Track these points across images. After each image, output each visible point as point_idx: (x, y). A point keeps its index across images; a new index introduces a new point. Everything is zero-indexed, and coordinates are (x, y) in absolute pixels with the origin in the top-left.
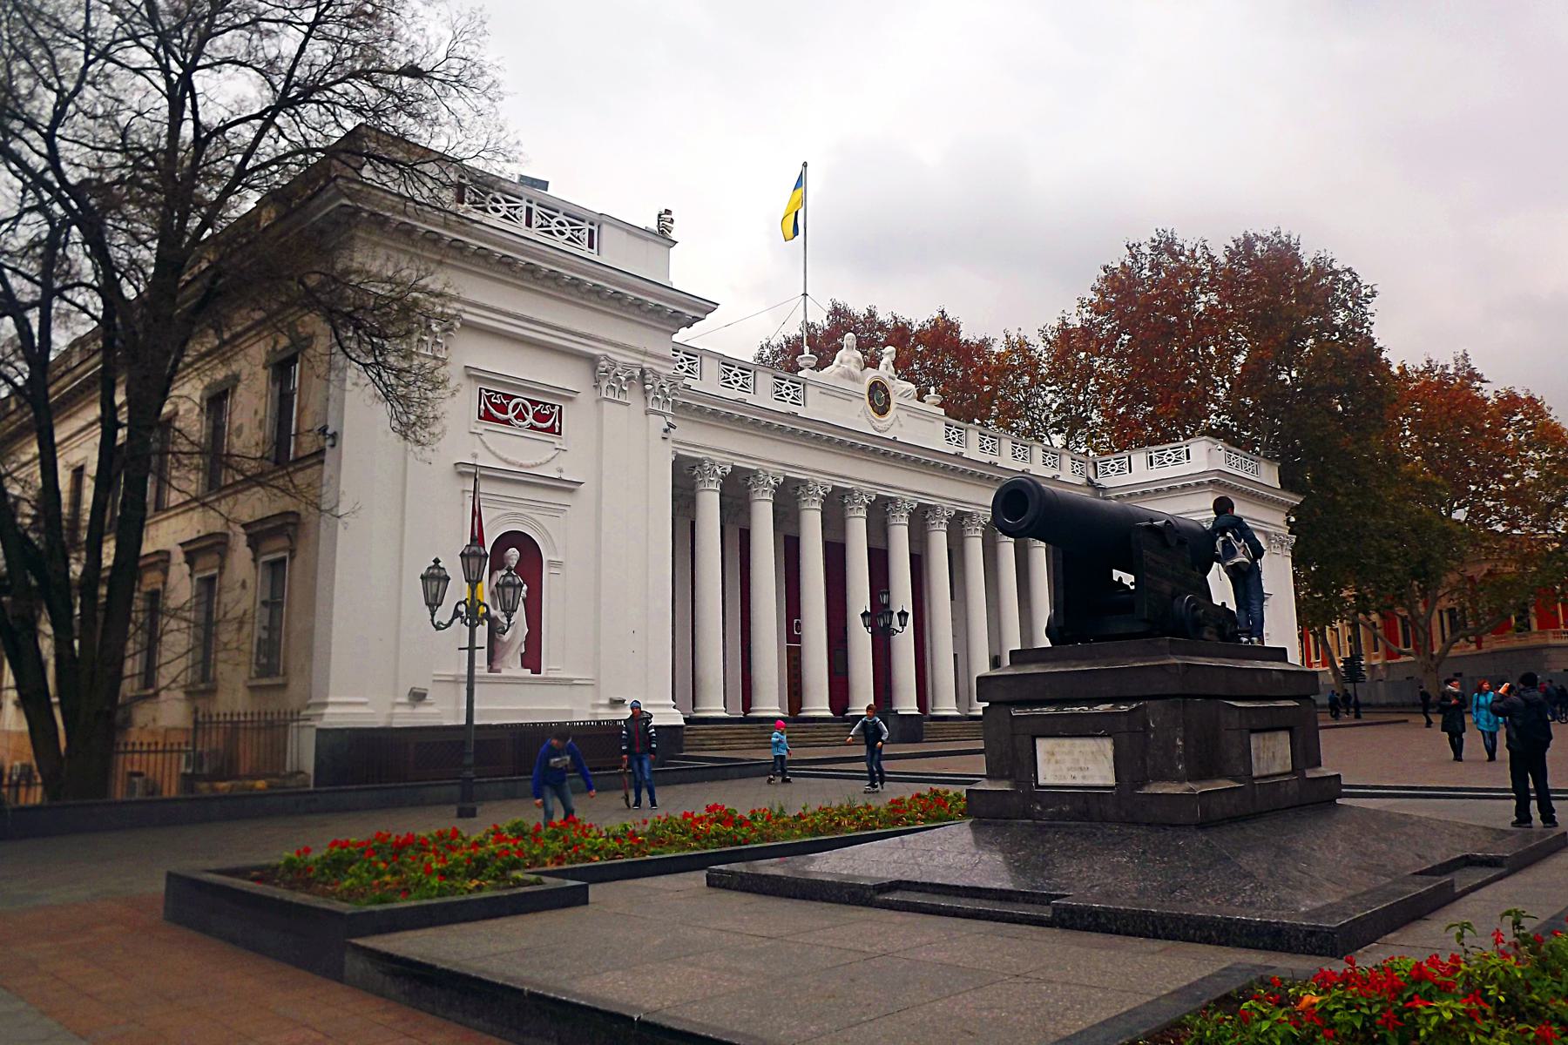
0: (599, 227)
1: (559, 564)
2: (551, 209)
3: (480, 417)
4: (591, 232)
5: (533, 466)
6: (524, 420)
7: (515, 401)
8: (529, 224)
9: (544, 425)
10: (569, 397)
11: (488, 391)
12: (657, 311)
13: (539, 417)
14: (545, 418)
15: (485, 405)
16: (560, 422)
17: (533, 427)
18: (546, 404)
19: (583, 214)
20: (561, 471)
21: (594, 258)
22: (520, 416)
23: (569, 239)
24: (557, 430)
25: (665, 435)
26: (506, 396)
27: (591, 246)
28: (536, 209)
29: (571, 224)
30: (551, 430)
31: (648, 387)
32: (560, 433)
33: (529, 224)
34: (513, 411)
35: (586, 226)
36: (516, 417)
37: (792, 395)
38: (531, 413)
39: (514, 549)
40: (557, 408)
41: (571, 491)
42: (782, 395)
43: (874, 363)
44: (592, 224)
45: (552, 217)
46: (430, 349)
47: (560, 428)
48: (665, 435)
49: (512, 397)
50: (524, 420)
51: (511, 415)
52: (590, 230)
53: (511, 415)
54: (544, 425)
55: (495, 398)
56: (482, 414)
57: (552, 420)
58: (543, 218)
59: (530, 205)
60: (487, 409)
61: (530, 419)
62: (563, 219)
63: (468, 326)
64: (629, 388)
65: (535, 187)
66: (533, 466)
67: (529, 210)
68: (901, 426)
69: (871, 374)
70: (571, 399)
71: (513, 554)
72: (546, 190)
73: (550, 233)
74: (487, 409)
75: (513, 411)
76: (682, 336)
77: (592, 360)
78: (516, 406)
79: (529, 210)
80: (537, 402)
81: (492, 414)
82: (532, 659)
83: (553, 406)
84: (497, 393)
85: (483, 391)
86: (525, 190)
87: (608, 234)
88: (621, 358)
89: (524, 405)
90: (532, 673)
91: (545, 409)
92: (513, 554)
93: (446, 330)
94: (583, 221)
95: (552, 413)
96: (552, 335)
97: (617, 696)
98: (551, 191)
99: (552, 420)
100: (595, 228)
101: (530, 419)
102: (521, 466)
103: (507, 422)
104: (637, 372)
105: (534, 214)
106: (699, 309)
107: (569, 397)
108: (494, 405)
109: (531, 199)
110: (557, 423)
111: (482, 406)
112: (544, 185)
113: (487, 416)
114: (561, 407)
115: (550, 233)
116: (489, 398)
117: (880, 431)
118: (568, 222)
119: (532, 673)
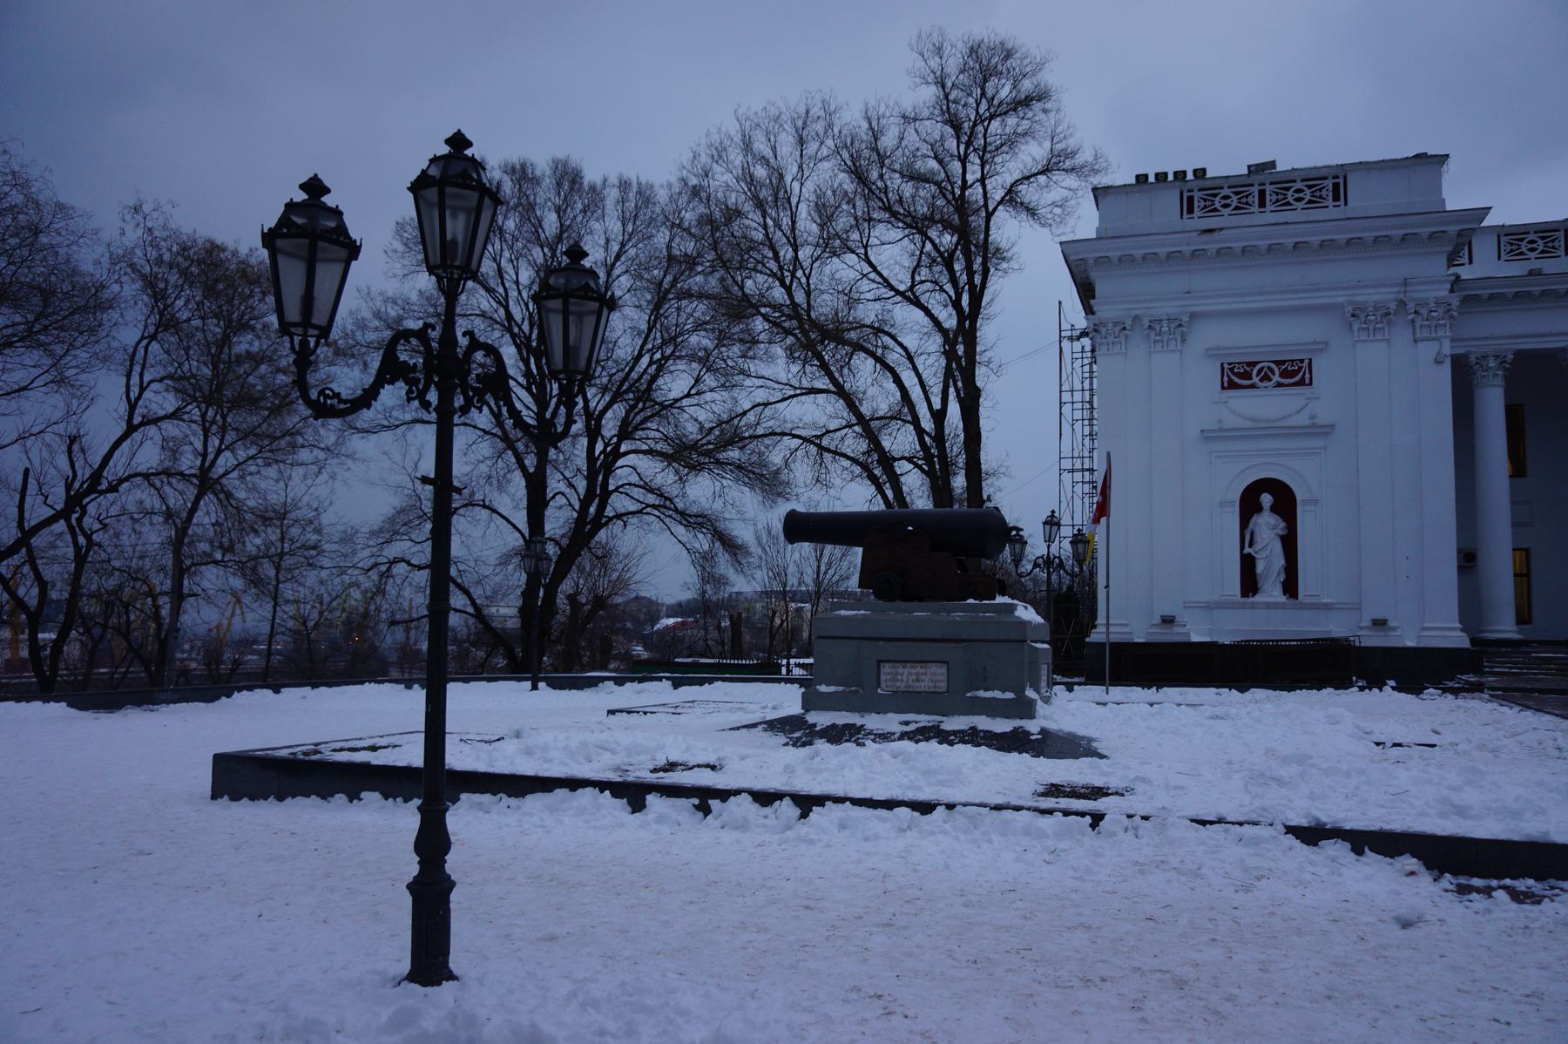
1: (1315, 502)
2: (1286, 183)
3: (1223, 388)
4: (1336, 186)
6: (1270, 380)
8: (1262, 204)
11: (1230, 364)
13: (1285, 374)
14: (1292, 374)
15: (1228, 376)
16: (1310, 373)
17: (1279, 385)
18: (1293, 361)
19: (1323, 173)
22: (1266, 378)
24: (1307, 381)
27: (1336, 198)
28: (1269, 189)
30: (1301, 383)
32: (1311, 384)
33: (1262, 204)
34: (1257, 376)
35: (1329, 183)
38: (1277, 373)
39: (1266, 494)
40: (1307, 361)
41: (1326, 434)
47: (1311, 379)
49: (1254, 364)
50: (1270, 380)
51: (1255, 380)
53: (1255, 380)
56: (1226, 385)
60: (1230, 381)
61: (1276, 378)
67: (1262, 193)
70: (1321, 350)
71: (1266, 499)
74: (1230, 381)
78: (1262, 369)
79: (1262, 193)
80: (1283, 362)
81: (1236, 383)
82: (1290, 586)
83: (1302, 361)
84: (1239, 363)
85: (1225, 365)
86: (1256, 179)
89: (1269, 368)
92: (1266, 499)
95: (1300, 369)
101: (1276, 378)
102: (1268, 421)
103: (1253, 386)
105: (1268, 193)
108: (1237, 375)
110: (1307, 376)
111: (1226, 379)
112: (1272, 164)
113: (1232, 386)
114: (1310, 360)
116: (1231, 370)
118: (1306, 186)
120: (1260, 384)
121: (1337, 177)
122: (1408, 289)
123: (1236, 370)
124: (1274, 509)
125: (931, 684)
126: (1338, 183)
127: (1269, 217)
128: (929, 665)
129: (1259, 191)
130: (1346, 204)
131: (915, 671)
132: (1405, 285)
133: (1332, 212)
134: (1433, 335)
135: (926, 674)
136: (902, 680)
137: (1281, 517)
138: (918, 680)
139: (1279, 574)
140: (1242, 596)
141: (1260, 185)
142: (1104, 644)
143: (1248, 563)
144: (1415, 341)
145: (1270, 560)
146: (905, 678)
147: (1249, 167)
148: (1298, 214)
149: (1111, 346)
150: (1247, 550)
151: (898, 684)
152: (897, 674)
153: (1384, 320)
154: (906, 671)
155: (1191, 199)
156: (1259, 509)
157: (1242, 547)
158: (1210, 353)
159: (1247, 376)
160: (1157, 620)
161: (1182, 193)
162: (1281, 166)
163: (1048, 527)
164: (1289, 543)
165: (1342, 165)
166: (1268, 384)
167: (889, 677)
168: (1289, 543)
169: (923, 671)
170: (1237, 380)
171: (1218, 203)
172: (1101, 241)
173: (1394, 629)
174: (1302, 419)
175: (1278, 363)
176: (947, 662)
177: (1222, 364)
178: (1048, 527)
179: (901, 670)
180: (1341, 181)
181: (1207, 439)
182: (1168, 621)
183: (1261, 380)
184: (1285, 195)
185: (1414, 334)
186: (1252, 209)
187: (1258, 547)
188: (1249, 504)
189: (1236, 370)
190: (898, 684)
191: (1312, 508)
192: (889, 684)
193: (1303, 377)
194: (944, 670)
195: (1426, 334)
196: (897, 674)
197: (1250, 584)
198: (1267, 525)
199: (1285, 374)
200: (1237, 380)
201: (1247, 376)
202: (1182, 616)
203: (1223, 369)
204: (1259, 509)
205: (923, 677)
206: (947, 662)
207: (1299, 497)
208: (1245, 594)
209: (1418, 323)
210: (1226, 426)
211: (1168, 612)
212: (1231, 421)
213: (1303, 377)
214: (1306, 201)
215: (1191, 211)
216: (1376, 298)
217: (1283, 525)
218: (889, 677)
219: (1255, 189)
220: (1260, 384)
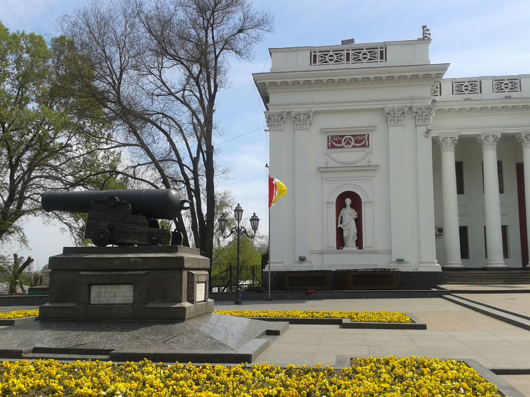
1: (370, 202)
2: (358, 50)
3: (328, 148)
4: (382, 52)
6: (350, 144)
7: (345, 137)
8: (348, 60)
9: (360, 145)
10: (373, 128)
11: (331, 136)
13: (357, 141)
14: (360, 141)
15: (331, 142)
16: (368, 141)
17: (354, 147)
19: (376, 46)
20: (370, 162)
22: (348, 143)
24: (367, 145)
25: (426, 135)
26: (341, 136)
27: (382, 58)
28: (351, 52)
30: (364, 146)
32: (368, 146)
33: (348, 60)
34: (344, 142)
35: (379, 50)
36: (346, 144)
38: (353, 141)
40: (367, 135)
45: (360, 53)
47: (368, 144)
48: (426, 135)
49: (342, 137)
50: (350, 144)
51: (343, 144)
52: (381, 51)
53: (343, 144)
54: (360, 145)
55: (336, 138)
56: (330, 146)
60: (332, 144)
61: (353, 143)
63: (315, 113)
64: (404, 118)
66: (355, 163)
67: (348, 54)
70: (374, 130)
71: (348, 201)
74: (332, 144)
75: (344, 142)
79: (348, 54)
80: (356, 136)
82: (359, 243)
83: (365, 135)
84: (336, 136)
85: (330, 137)
88: (395, 105)
89: (349, 138)
91: (360, 138)
92: (348, 201)
95: (364, 139)
96: (369, 105)
97: (400, 258)
98: (356, 42)
100: (384, 50)
101: (353, 143)
102: (349, 164)
103: (342, 147)
104: (406, 110)
105: (350, 55)
106: (444, 67)
107: (373, 128)
108: (335, 141)
110: (367, 142)
111: (330, 143)
112: (352, 41)
113: (333, 147)
114: (368, 135)
116: (332, 139)
121: (382, 48)
123: (334, 139)
124: (352, 206)
126: (383, 51)
127: (351, 65)
129: (347, 53)
130: (386, 61)
133: (379, 64)
134: (424, 123)
137: (355, 210)
139: (354, 237)
143: (340, 232)
145: (350, 231)
147: (342, 41)
148: (365, 64)
150: (339, 226)
153: (402, 115)
155: (315, 56)
156: (345, 206)
157: (337, 224)
158: (323, 131)
159: (339, 142)
160: (297, 259)
161: (311, 53)
165: (384, 42)
168: (358, 222)
171: (327, 58)
172: (271, 74)
174: (364, 163)
175: (354, 136)
177: (328, 136)
180: (384, 50)
181: (322, 172)
182: (302, 259)
183: (346, 144)
185: (416, 123)
186: (343, 62)
187: (344, 223)
188: (340, 203)
189: (334, 139)
191: (369, 205)
193: (365, 144)
195: (421, 123)
197: (341, 242)
198: (349, 214)
199: (357, 141)
201: (339, 142)
202: (309, 258)
204: (345, 206)
207: (363, 200)
208: (338, 248)
209: (417, 118)
210: (329, 166)
211: (303, 255)
212: (331, 164)
213: (365, 144)
214: (368, 59)
215: (315, 62)
216: (400, 105)
217: (356, 213)
219: (345, 53)
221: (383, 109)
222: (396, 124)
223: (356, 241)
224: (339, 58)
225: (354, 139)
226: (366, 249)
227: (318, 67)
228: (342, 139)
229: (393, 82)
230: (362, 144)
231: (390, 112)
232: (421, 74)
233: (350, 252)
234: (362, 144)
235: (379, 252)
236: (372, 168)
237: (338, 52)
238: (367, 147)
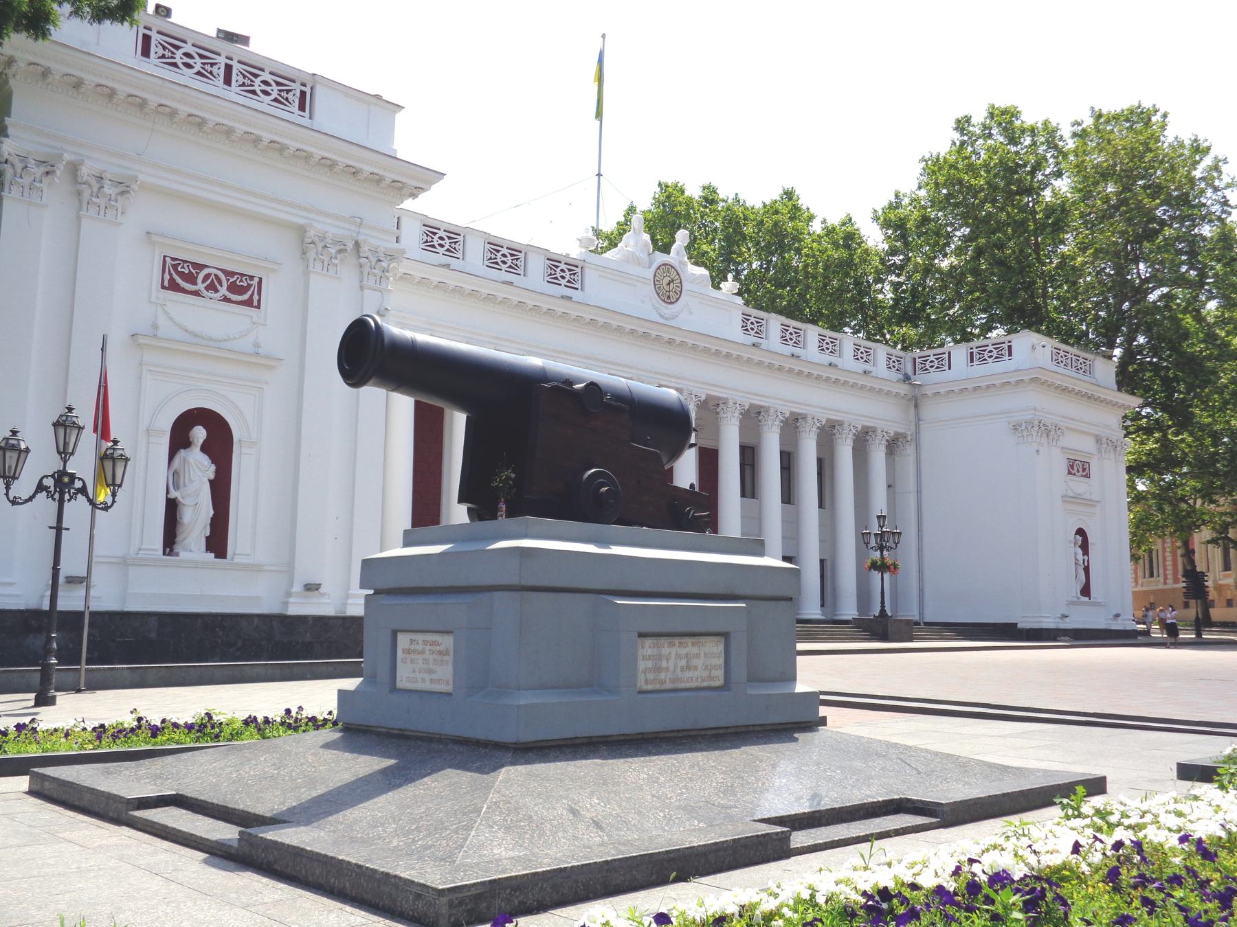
0: (312, 88)
2: (253, 69)
3: (163, 287)
4: (303, 94)
5: (225, 340)
6: (217, 291)
7: (206, 271)
8: (228, 81)
9: (240, 298)
11: (173, 259)
12: (376, 180)
13: (233, 288)
14: (240, 290)
16: (259, 294)
17: (226, 299)
18: (242, 275)
20: (257, 345)
21: (306, 121)
22: (212, 288)
23: (276, 100)
24: (255, 303)
26: (196, 266)
27: (302, 107)
28: (236, 67)
29: (278, 84)
30: (248, 303)
31: (363, 261)
32: (258, 307)
33: (228, 81)
34: (203, 282)
35: (297, 88)
36: (207, 288)
37: (568, 278)
38: (225, 284)
39: (200, 428)
40: (256, 280)
41: (270, 368)
42: (556, 278)
43: (666, 249)
44: (304, 85)
45: (256, 76)
46: (102, 212)
49: (201, 267)
50: (217, 291)
51: (201, 286)
53: (201, 286)
54: (240, 298)
55: (183, 267)
56: (166, 284)
57: (249, 293)
58: (244, 77)
59: (229, 62)
60: (172, 280)
61: (223, 291)
62: (269, 78)
65: (236, 42)
66: (225, 340)
67: (229, 68)
68: (691, 313)
69: (661, 258)
70: (273, 271)
71: (199, 434)
72: (248, 46)
73: (254, 92)
74: (172, 280)
76: (408, 204)
77: (301, 231)
78: (207, 276)
79: (229, 68)
80: (231, 274)
82: (217, 543)
83: (252, 278)
85: (168, 260)
86: (226, 47)
87: (322, 100)
88: (332, 229)
89: (216, 276)
90: (216, 557)
91: (241, 281)
92: (199, 434)
93: (123, 193)
94: (294, 81)
95: (249, 286)
98: (254, 47)
99: (249, 293)
100: (308, 90)
101: (223, 291)
103: (196, 293)
104: (350, 245)
105: (234, 72)
108: (181, 275)
109: (230, 55)
110: (256, 297)
111: (167, 277)
112: (244, 40)
113: (173, 287)
114: (261, 279)
115: (254, 92)
116: (175, 267)
117: (666, 319)
119: (216, 557)
120: (205, 293)
121: (304, 85)
122: (362, 230)
124: (204, 449)
125: (705, 674)
128: (703, 639)
131: (683, 651)
132: (360, 225)
135: (697, 656)
136: (667, 669)
137: (210, 458)
138: (688, 668)
140: (164, 554)
141: (226, 58)
142: (80, 615)
143: (172, 507)
144: (362, 288)
146: (671, 665)
147: (219, 31)
149: (26, 191)
150: (174, 494)
151: (663, 676)
152: (660, 657)
154: (674, 651)
156: (187, 444)
157: (168, 492)
159: (191, 279)
162: (254, 47)
163: (61, 431)
164: (221, 489)
165: (314, 74)
166: (214, 295)
167: (650, 664)
168: (221, 489)
169: (695, 650)
170: (179, 280)
173: (323, 595)
175: (229, 274)
176: (725, 635)
177: (165, 257)
178: (61, 431)
179: (666, 651)
183: (207, 288)
184: (252, 81)
186: (216, 82)
188: (179, 439)
190: (663, 676)
192: (651, 676)
194: (720, 648)
196: (660, 657)
198: (199, 467)
200: (179, 280)
201: (191, 279)
203: (164, 261)
205: (694, 662)
206: (725, 635)
207: (236, 435)
215: (146, 52)
217: (213, 468)
218: (650, 664)
219: (222, 61)
220: (205, 293)
221: (301, 231)
222: (325, 272)
223: (207, 538)
224: (206, 67)
225: (228, 280)
226: (236, 560)
227: (152, 66)
228: (197, 273)
229: (329, 174)
230: (246, 297)
231: (316, 239)
232: (390, 176)
233: (196, 565)
234: (246, 297)
235: (265, 568)
236: (259, 359)
237: (206, 53)
238: (255, 307)
